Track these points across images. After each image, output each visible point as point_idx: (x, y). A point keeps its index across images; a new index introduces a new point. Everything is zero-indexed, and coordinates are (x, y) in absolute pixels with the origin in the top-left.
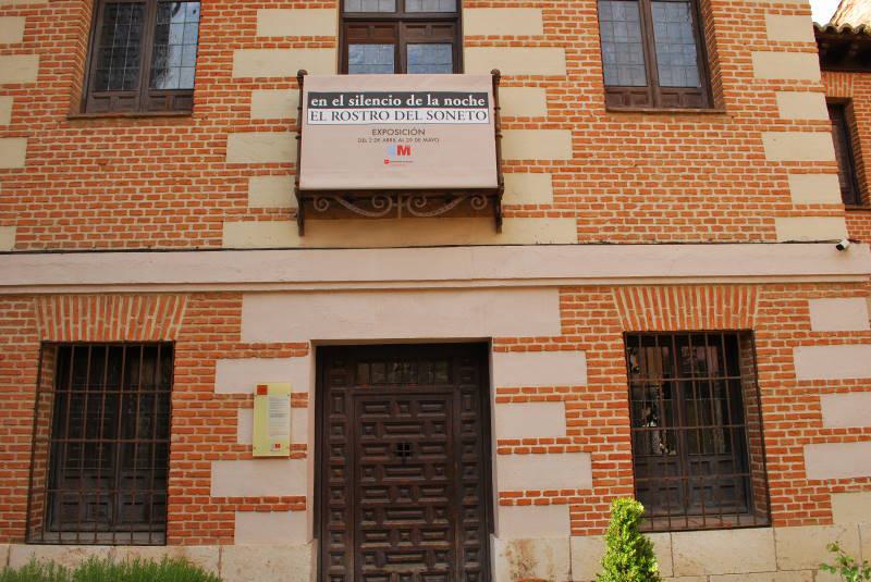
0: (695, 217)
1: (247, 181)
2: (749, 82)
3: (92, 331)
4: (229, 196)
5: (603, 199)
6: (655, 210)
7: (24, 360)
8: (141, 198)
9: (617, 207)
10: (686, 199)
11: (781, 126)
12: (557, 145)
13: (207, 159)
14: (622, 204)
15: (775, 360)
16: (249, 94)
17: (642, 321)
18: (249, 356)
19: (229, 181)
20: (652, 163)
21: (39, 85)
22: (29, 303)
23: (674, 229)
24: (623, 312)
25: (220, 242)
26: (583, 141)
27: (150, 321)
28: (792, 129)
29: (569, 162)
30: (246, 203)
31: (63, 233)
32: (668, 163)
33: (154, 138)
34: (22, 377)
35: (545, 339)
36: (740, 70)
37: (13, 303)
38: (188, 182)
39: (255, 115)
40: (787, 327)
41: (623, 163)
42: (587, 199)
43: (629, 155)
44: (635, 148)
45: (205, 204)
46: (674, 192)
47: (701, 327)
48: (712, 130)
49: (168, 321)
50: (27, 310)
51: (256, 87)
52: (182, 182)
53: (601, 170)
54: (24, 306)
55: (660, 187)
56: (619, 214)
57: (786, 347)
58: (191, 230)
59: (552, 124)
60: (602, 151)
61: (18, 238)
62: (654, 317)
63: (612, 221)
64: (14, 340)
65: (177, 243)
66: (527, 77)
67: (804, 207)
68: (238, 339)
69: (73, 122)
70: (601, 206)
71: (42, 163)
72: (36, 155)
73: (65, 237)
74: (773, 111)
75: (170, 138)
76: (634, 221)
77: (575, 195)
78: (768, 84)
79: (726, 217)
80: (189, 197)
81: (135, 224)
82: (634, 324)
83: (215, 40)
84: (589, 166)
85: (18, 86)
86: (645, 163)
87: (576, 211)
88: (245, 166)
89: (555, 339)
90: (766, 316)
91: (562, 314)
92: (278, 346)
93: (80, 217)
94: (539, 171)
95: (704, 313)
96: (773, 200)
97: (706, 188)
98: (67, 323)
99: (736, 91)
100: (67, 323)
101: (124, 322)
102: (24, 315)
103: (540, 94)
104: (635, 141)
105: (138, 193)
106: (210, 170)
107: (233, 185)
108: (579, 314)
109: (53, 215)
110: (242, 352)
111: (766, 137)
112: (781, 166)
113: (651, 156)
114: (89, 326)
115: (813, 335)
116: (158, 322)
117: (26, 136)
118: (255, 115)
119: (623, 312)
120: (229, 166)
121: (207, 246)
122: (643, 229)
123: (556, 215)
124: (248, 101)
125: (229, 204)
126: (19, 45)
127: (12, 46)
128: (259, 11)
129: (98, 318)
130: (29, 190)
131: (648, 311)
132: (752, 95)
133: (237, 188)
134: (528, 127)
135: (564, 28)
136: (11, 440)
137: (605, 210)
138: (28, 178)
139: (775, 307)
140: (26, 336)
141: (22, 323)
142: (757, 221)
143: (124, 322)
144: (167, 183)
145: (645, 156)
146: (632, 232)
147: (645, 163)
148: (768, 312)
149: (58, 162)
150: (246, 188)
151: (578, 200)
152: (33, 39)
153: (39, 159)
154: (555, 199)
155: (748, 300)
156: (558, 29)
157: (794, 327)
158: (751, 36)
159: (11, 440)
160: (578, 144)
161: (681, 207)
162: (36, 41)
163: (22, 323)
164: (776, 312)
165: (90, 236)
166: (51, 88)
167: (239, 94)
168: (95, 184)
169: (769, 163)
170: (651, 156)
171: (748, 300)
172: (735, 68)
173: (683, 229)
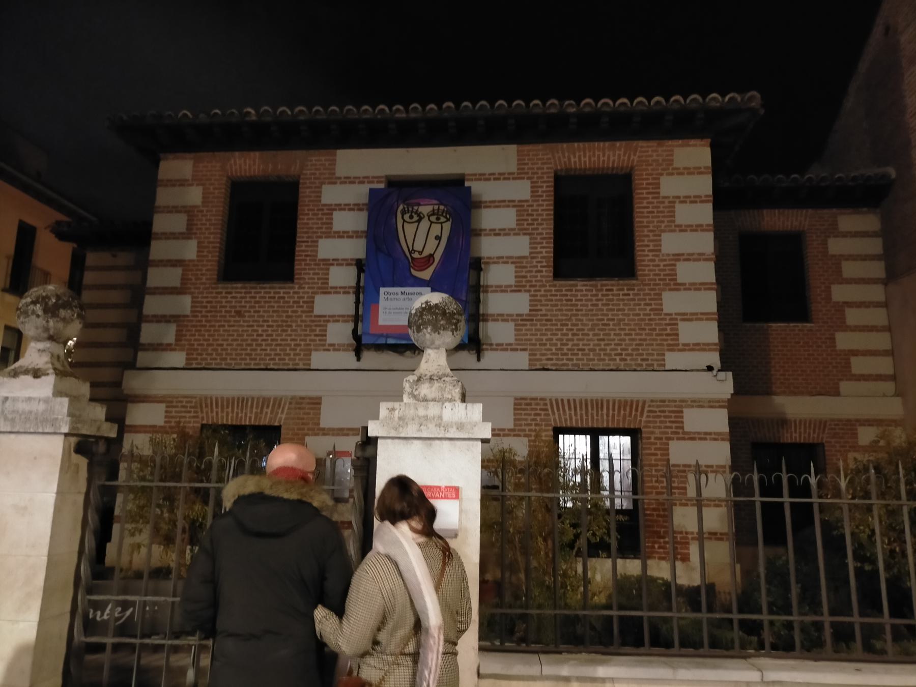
0: (608, 351)
1: (326, 326)
2: (657, 256)
3: (232, 417)
4: (316, 335)
5: (547, 340)
6: (581, 347)
8: (262, 335)
9: (556, 345)
10: (603, 340)
11: (678, 287)
12: (520, 303)
13: (302, 312)
14: (559, 343)
15: (656, 449)
16: (328, 269)
17: (566, 420)
18: (324, 434)
19: (316, 326)
20: (582, 315)
23: (594, 360)
24: (554, 414)
25: (310, 365)
26: (536, 301)
27: (267, 413)
28: (685, 289)
29: (527, 315)
30: (325, 340)
31: (214, 356)
32: (592, 315)
33: (270, 297)
35: (503, 430)
36: (651, 248)
38: (291, 326)
40: (666, 427)
41: (562, 315)
42: (536, 340)
43: (566, 310)
44: (571, 305)
45: (301, 340)
46: (594, 335)
47: (605, 426)
48: (626, 292)
49: (277, 413)
51: (333, 265)
52: (287, 326)
53: (547, 320)
54: (191, 402)
55: (586, 332)
56: (557, 349)
57: (664, 441)
58: (292, 356)
59: (518, 288)
60: (548, 308)
62: (574, 418)
63: (553, 354)
65: (284, 364)
66: (502, 257)
67: (688, 345)
68: (319, 424)
70: (545, 345)
71: (201, 312)
73: (216, 359)
74: (673, 275)
75: (279, 298)
76: (566, 354)
77: (529, 337)
78: (671, 257)
79: (630, 352)
80: (290, 335)
81: (259, 352)
82: (561, 421)
83: (306, 233)
84: (539, 317)
86: (577, 315)
87: (528, 347)
88: (325, 316)
89: (509, 430)
90: (651, 419)
91: (515, 414)
92: (342, 429)
93: (225, 347)
94: (507, 320)
95: (608, 415)
96: (666, 340)
97: (618, 332)
98: (217, 413)
99: (646, 263)
100: (217, 413)
101: (251, 412)
102: (191, 407)
104: (571, 300)
105: (260, 332)
106: (304, 318)
107: (318, 329)
108: (525, 414)
109: (208, 345)
110: (321, 432)
111: (666, 295)
112: (674, 316)
113: (582, 310)
114: (230, 415)
115: (684, 433)
116: (272, 413)
119: (554, 414)
120: (316, 316)
121: (301, 366)
122: (572, 360)
123: (516, 350)
124: (328, 274)
125: (314, 340)
128: (335, 213)
129: (235, 410)
131: (570, 414)
132: (658, 266)
133: (320, 330)
134: (502, 291)
135: (530, 222)
137: (548, 346)
139: (659, 414)
142: (653, 355)
143: (251, 412)
144: (278, 326)
145: (577, 310)
146: (565, 362)
147: (577, 315)
148: (654, 417)
149: (211, 312)
150: (326, 331)
151: (530, 340)
154: (516, 340)
155: (640, 409)
156: (525, 223)
157: (671, 427)
158: (663, 222)
160: (534, 301)
161: (599, 345)
163: (190, 412)
164: (659, 417)
165: (231, 359)
167: (322, 269)
168: (233, 326)
169: (666, 314)
170: (582, 310)
171: (640, 409)
172: (648, 246)
173: (599, 360)
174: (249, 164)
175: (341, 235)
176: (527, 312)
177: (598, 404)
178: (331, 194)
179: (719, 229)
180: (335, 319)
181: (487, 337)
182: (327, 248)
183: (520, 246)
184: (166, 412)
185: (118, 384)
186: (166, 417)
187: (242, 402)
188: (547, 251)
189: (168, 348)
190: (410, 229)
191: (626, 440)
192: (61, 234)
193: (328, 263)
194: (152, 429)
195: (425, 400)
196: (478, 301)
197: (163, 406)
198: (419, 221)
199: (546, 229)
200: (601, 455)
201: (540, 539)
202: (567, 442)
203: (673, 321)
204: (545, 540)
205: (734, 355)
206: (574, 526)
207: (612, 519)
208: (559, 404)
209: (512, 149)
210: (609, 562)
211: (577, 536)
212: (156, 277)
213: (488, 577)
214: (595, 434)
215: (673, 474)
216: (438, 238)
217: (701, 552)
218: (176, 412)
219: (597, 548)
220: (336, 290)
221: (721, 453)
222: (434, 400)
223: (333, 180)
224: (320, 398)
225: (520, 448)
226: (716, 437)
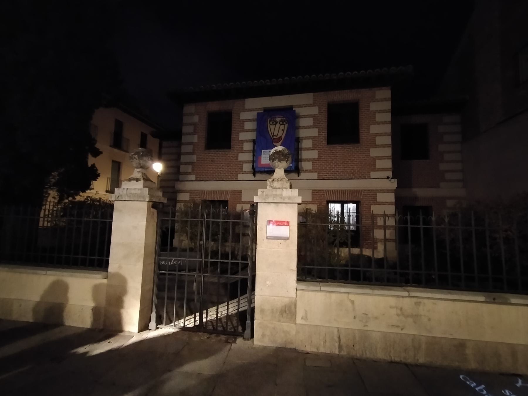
12: (314, 154)
39: (244, 149)
59: (313, 149)
103: (311, 141)
118: (244, 149)
160: (319, 154)
174: (214, 106)
175: (247, 131)
176: (317, 157)
177: (344, 192)
178: (244, 116)
179: (393, 122)
180: (246, 162)
181: (302, 168)
182: (243, 136)
183: (314, 132)
185: (174, 187)
187: (215, 192)
188: (325, 134)
189: (189, 174)
190: (272, 127)
191: (355, 205)
192: (154, 135)
193: (243, 141)
194: (185, 202)
195: (276, 188)
196: (298, 154)
197: (188, 194)
198: (276, 124)
199: (324, 124)
200: (345, 211)
201: (321, 241)
202: (331, 206)
203: (374, 159)
204: (323, 241)
205: (397, 172)
206: (334, 236)
207: (349, 235)
208: (329, 192)
209: (311, 95)
210: (347, 250)
211: (335, 240)
212: (185, 149)
213: (302, 254)
214: (342, 203)
215: (374, 217)
216: (283, 130)
217: (382, 245)
219: (343, 244)
220: (245, 152)
221: (391, 210)
222: (279, 188)
223: (244, 110)
224: (241, 191)
225: (314, 208)
226: (390, 203)
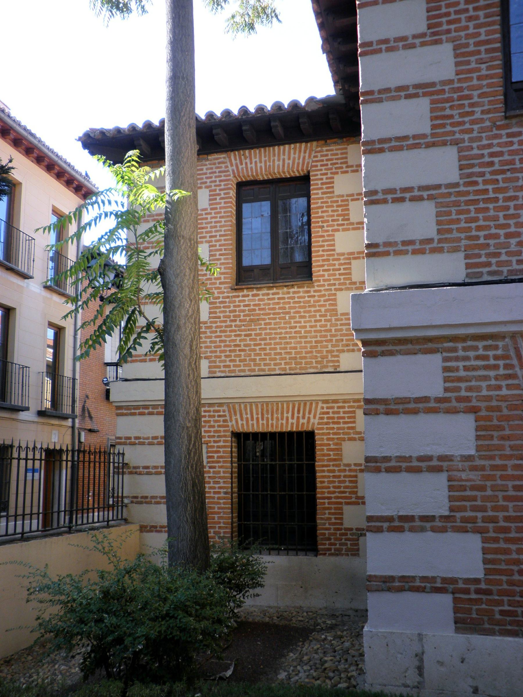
7: (505, 412)
21: (459, 80)
22: (500, 344)
34: (507, 432)
37: (481, 344)
50: (499, 352)
54: (496, 348)
61: (468, 266)
64: (489, 388)
69: (514, 121)
71: (482, 174)
72: (473, 166)
85: (433, 84)
109: (508, 236)
117: (455, 143)
126: (423, 35)
127: (415, 37)
130: (472, 208)
136: (505, 509)
138: (468, 193)
140: (504, 383)
141: (496, 367)
149: (503, 172)
152: (440, 24)
153: (476, 169)
159: (505, 509)
162: (445, 27)
163: (496, 367)
166: (475, 82)
184: (446, 369)
186: (446, 380)
218: (466, 368)
